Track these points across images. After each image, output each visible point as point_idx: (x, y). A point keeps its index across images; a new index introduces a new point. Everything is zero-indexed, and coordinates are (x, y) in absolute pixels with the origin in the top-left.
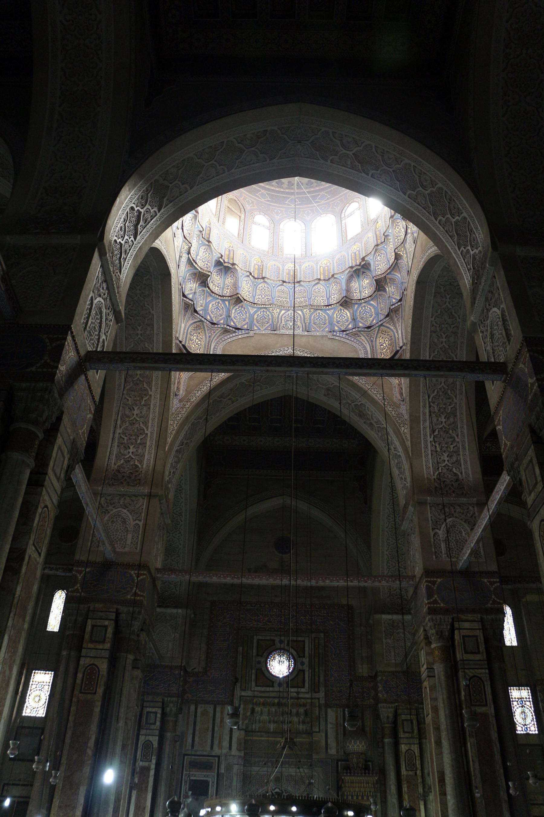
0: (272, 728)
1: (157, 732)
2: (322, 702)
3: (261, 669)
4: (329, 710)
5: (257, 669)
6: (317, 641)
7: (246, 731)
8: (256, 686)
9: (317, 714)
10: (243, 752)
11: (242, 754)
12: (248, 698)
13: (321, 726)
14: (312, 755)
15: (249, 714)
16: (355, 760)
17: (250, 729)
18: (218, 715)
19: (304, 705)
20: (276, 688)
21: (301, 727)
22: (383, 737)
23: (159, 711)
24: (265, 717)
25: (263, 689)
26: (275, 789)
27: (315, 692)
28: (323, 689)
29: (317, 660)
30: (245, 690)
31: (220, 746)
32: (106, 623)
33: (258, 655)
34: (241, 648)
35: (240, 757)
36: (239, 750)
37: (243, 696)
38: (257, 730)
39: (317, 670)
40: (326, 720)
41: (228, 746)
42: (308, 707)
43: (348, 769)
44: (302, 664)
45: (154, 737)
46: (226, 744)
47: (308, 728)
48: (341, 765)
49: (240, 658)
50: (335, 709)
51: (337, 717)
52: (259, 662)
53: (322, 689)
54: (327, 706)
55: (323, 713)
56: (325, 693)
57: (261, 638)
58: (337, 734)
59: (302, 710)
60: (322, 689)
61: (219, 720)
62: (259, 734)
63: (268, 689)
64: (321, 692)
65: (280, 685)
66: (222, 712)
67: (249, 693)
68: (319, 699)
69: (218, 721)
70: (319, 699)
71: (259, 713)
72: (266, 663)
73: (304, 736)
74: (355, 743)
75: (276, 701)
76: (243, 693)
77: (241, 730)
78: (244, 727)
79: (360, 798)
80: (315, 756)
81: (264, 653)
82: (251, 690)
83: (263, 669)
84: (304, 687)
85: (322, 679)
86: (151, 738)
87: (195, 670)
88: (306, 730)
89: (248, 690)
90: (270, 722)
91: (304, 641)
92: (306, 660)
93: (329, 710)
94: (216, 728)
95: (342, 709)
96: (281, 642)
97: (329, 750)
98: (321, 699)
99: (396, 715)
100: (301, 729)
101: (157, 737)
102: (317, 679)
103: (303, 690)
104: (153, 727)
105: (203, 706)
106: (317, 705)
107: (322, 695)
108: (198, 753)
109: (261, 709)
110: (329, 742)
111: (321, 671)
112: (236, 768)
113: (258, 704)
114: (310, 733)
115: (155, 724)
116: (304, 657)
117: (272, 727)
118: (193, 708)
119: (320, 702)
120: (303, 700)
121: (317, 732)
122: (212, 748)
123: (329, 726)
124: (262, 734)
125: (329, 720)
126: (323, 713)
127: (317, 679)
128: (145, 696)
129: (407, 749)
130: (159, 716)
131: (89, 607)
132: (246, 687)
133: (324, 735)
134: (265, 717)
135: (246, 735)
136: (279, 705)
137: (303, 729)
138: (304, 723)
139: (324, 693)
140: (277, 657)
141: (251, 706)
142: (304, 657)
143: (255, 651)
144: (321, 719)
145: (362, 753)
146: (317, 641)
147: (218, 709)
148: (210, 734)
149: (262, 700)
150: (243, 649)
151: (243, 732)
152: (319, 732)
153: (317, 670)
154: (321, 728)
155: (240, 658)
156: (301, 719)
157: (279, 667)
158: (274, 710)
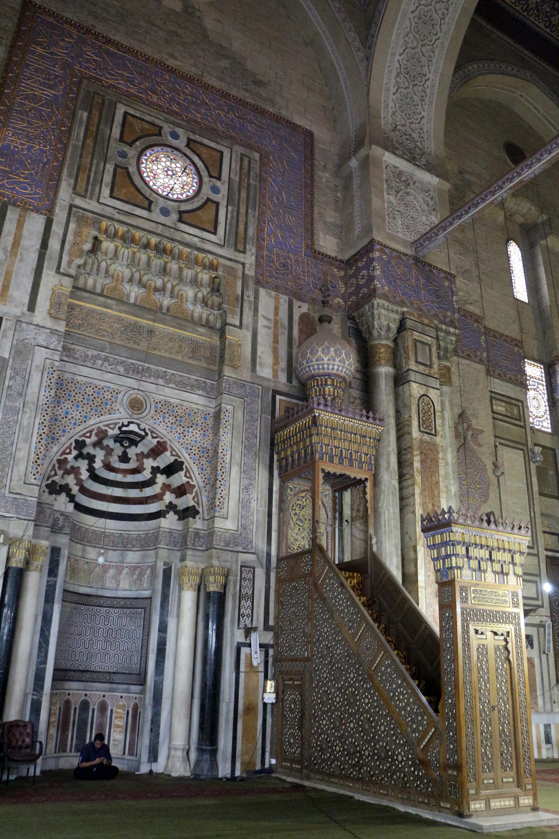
0: (133, 295)
2: (250, 272)
3: (127, 168)
4: (262, 292)
5: (116, 166)
6: (246, 162)
8: (111, 196)
9: (239, 292)
11: (61, 327)
12: (90, 215)
13: (244, 316)
17: (81, 283)
19: (213, 267)
20: (156, 215)
21: (198, 310)
24: (120, 269)
25: (127, 207)
26: (129, 423)
27: (237, 250)
28: (254, 250)
29: (244, 194)
34: (85, 114)
35: (53, 332)
36: (54, 317)
37: (76, 207)
38: (98, 290)
39: (243, 210)
40: (256, 310)
41: (26, 300)
42: (220, 272)
44: (215, 190)
47: (211, 318)
48: (281, 400)
50: (273, 293)
51: (276, 309)
52: (124, 155)
53: (251, 249)
54: (258, 283)
55: (250, 293)
56: (256, 257)
57: (132, 111)
58: (276, 340)
62: (102, 299)
63: (138, 211)
64: (248, 253)
66: (20, 225)
67: (93, 205)
68: (243, 264)
70: (243, 264)
71: (111, 255)
72: (138, 163)
73: (201, 330)
75: (154, 240)
76: (79, 201)
77: (64, 275)
78: (73, 272)
80: (227, 371)
82: (98, 202)
83: (131, 170)
84: (215, 233)
85: (251, 231)
88: (208, 320)
89: (91, 198)
90: (131, 280)
91: (222, 153)
92: (224, 188)
93: (262, 292)
95: (286, 298)
96: (175, 136)
97: (258, 368)
98: (247, 266)
99: (402, 327)
102: (242, 227)
106: (240, 274)
107: (250, 259)
109: (117, 247)
110: (259, 353)
111: (250, 217)
112: (40, 356)
113: (114, 236)
116: (219, 178)
117: (134, 293)
120: (211, 257)
123: (262, 322)
124: (109, 301)
125: (261, 311)
126: (250, 293)
127: (242, 227)
129: (422, 393)
132: (86, 191)
133: (249, 335)
134: (120, 269)
135: (72, 295)
136: (160, 250)
137: (200, 318)
138: (204, 302)
139: (254, 257)
140: (164, 159)
142: (219, 178)
143: (116, 131)
144: (246, 304)
146: (246, 162)
149: (122, 229)
150: (89, 118)
151: (67, 282)
152: (241, 327)
153: (243, 210)
154: (245, 321)
155: (79, 132)
156: (200, 295)
157: (167, 175)
158: (144, 258)
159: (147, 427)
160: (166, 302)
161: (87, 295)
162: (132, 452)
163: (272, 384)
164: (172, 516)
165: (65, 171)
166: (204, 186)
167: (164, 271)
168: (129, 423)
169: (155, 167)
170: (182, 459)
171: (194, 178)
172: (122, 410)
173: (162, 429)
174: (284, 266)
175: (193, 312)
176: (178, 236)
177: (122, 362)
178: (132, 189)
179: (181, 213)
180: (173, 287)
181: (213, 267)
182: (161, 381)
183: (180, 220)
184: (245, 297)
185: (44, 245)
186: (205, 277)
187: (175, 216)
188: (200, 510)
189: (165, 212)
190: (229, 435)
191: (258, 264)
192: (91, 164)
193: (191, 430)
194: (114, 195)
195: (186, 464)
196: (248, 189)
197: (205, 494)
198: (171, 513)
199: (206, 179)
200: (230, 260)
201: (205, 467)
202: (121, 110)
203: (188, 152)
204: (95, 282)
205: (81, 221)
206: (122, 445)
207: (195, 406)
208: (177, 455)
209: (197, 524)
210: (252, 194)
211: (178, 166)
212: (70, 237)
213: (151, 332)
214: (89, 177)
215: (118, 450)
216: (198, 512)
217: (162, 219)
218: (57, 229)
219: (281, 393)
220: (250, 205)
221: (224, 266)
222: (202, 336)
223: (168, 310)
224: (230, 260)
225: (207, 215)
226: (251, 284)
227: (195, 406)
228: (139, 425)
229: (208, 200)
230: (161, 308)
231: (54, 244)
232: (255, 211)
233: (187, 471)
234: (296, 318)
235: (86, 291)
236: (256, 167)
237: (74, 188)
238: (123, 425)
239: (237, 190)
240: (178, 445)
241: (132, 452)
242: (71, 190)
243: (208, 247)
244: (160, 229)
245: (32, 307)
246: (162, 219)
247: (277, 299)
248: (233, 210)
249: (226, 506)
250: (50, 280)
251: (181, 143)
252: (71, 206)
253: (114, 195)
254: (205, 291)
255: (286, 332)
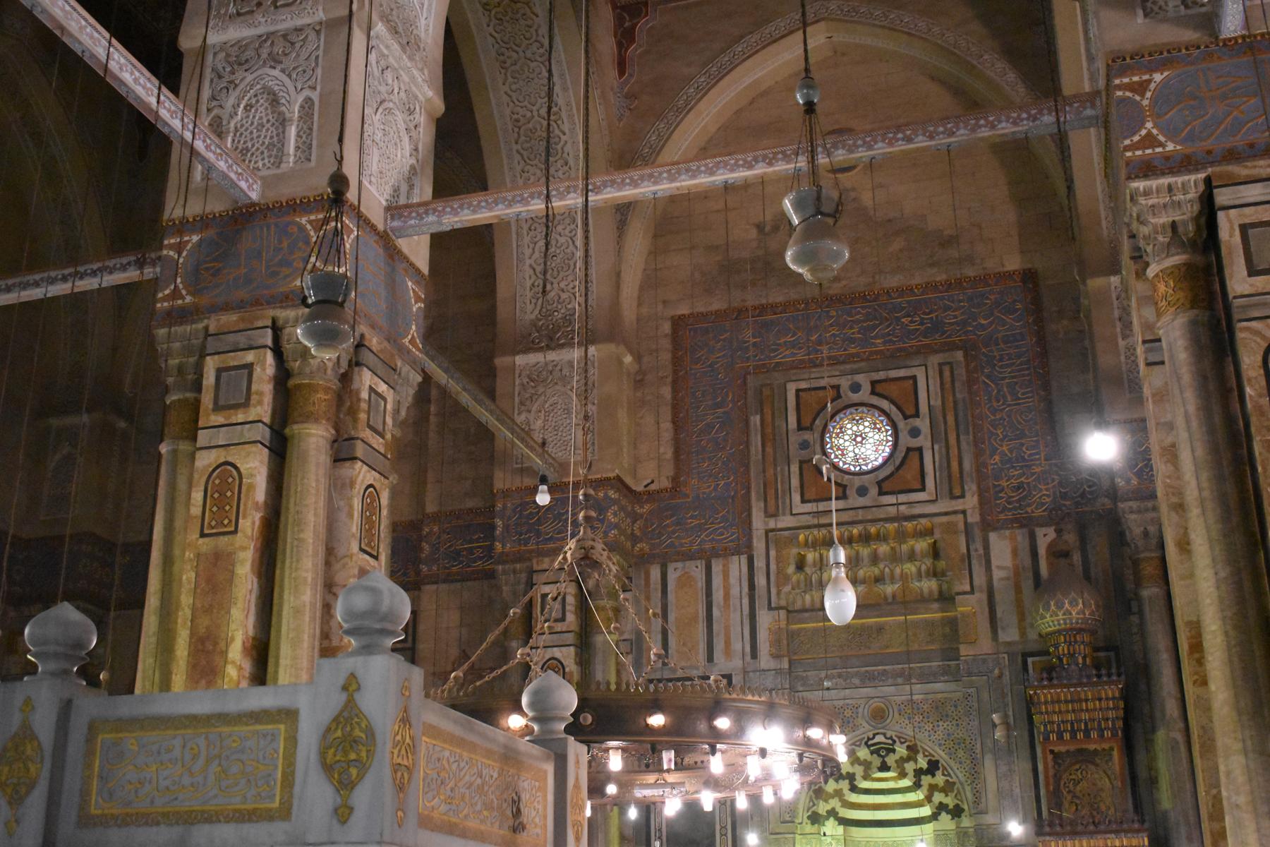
1: (570, 638)
2: (974, 518)
4: (993, 536)
6: (947, 374)
7: (789, 611)
8: (803, 501)
10: (786, 660)
12: (786, 533)
14: (958, 649)
15: (791, 569)
16: (1063, 648)
17: (798, 605)
18: (717, 581)
19: (929, 532)
22: (1138, 583)
23: (572, 589)
27: (953, 497)
28: (974, 487)
30: (775, 515)
31: (728, 652)
32: (250, 357)
33: (800, 428)
34: (758, 417)
35: (779, 671)
36: (776, 656)
37: (773, 530)
42: (937, 535)
43: (1050, 672)
44: (915, 433)
45: (564, 649)
46: (740, 644)
49: (756, 440)
50: (1007, 532)
53: (971, 487)
54: (987, 525)
55: (978, 545)
56: (980, 496)
57: (804, 385)
59: (922, 545)
60: (971, 487)
61: (721, 593)
64: (968, 495)
65: (862, 491)
67: (786, 521)
68: (964, 512)
69: (718, 596)
70: (964, 512)
74: (1060, 606)
77: (779, 608)
78: (783, 603)
79: (1080, 736)
80: (964, 650)
81: (814, 420)
84: (923, 489)
85: (967, 465)
86: (557, 653)
87: (653, 487)
88: (940, 592)
89: (784, 514)
91: (914, 378)
92: (923, 424)
93: (993, 536)
94: (716, 612)
96: (856, 388)
97: (1000, 631)
100: (926, 591)
101: (572, 649)
102: (955, 465)
103: (921, 496)
104: (559, 627)
105: (679, 565)
106: (961, 526)
107: (970, 501)
108: (680, 674)
110: (999, 615)
111: (964, 445)
114: (946, 599)
115: (563, 619)
116: (917, 415)
118: (655, 573)
119: (970, 520)
120: (923, 521)
121: (965, 593)
122: (710, 658)
125: (994, 562)
126: (978, 545)
127: (955, 465)
128: (534, 561)
130: (570, 600)
131: (206, 328)
137: (931, 592)
139: (976, 499)
140: (849, 426)
141: (794, 551)
142: (917, 415)
144: (974, 562)
145: (1080, 631)
146: (947, 374)
147: (717, 567)
148: (701, 627)
152: (972, 592)
155: (756, 440)
156: (924, 568)
159: (894, 734)
160: (889, 589)
161: (806, 615)
162: (891, 760)
163: (1020, 647)
164: (945, 817)
165: (753, 494)
166: (900, 435)
167: (875, 559)
168: (874, 735)
169: (841, 441)
170: (937, 758)
171: (887, 431)
172: (865, 724)
173: (909, 732)
174: (1019, 488)
175: (921, 589)
176: (880, 513)
177: (857, 674)
178: (819, 482)
179: (879, 483)
180: (892, 571)
181: (929, 532)
182: (900, 680)
183: (881, 493)
184: (973, 553)
185: (752, 586)
186: (922, 545)
187: (874, 491)
188: (966, 807)
189: (862, 491)
190: (976, 723)
191: (983, 502)
192: (775, 475)
193: (941, 723)
194: (806, 498)
195: (942, 761)
196: (955, 408)
197: (968, 789)
198: (944, 814)
199: (901, 425)
200: (946, 514)
201: (963, 760)
202: (791, 388)
203: (875, 400)
204: (812, 597)
205: (780, 544)
206: (879, 755)
207: (940, 696)
208: (931, 755)
209: (966, 822)
210: (961, 414)
211: (865, 427)
212: (773, 567)
213: (880, 629)
214: (777, 490)
215: (877, 761)
216: (963, 810)
217: (861, 501)
218: (760, 563)
219: (1032, 654)
220: (962, 427)
221: (941, 524)
222: (933, 614)
223: (894, 596)
224: (946, 514)
225: (910, 474)
226: (977, 532)
227: (940, 696)
228: (884, 735)
229: (909, 450)
230: (886, 598)
231: (761, 581)
232: (968, 434)
233: (945, 769)
234: (1042, 551)
235: (806, 611)
236: (961, 372)
237: (766, 511)
238: (869, 739)
239: (941, 418)
240: (930, 744)
241: (891, 760)
242: (762, 514)
243: (918, 510)
244: (861, 515)
245: (754, 655)
246: (861, 501)
247: (1013, 539)
248: (940, 448)
249: (983, 800)
250: (765, 620)
251: (864, 395)
252: (767, 532)
253: (806, 498)
254: (929, 562)
255: (1031, 574)
